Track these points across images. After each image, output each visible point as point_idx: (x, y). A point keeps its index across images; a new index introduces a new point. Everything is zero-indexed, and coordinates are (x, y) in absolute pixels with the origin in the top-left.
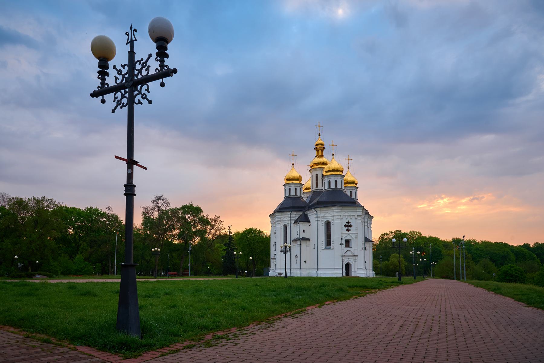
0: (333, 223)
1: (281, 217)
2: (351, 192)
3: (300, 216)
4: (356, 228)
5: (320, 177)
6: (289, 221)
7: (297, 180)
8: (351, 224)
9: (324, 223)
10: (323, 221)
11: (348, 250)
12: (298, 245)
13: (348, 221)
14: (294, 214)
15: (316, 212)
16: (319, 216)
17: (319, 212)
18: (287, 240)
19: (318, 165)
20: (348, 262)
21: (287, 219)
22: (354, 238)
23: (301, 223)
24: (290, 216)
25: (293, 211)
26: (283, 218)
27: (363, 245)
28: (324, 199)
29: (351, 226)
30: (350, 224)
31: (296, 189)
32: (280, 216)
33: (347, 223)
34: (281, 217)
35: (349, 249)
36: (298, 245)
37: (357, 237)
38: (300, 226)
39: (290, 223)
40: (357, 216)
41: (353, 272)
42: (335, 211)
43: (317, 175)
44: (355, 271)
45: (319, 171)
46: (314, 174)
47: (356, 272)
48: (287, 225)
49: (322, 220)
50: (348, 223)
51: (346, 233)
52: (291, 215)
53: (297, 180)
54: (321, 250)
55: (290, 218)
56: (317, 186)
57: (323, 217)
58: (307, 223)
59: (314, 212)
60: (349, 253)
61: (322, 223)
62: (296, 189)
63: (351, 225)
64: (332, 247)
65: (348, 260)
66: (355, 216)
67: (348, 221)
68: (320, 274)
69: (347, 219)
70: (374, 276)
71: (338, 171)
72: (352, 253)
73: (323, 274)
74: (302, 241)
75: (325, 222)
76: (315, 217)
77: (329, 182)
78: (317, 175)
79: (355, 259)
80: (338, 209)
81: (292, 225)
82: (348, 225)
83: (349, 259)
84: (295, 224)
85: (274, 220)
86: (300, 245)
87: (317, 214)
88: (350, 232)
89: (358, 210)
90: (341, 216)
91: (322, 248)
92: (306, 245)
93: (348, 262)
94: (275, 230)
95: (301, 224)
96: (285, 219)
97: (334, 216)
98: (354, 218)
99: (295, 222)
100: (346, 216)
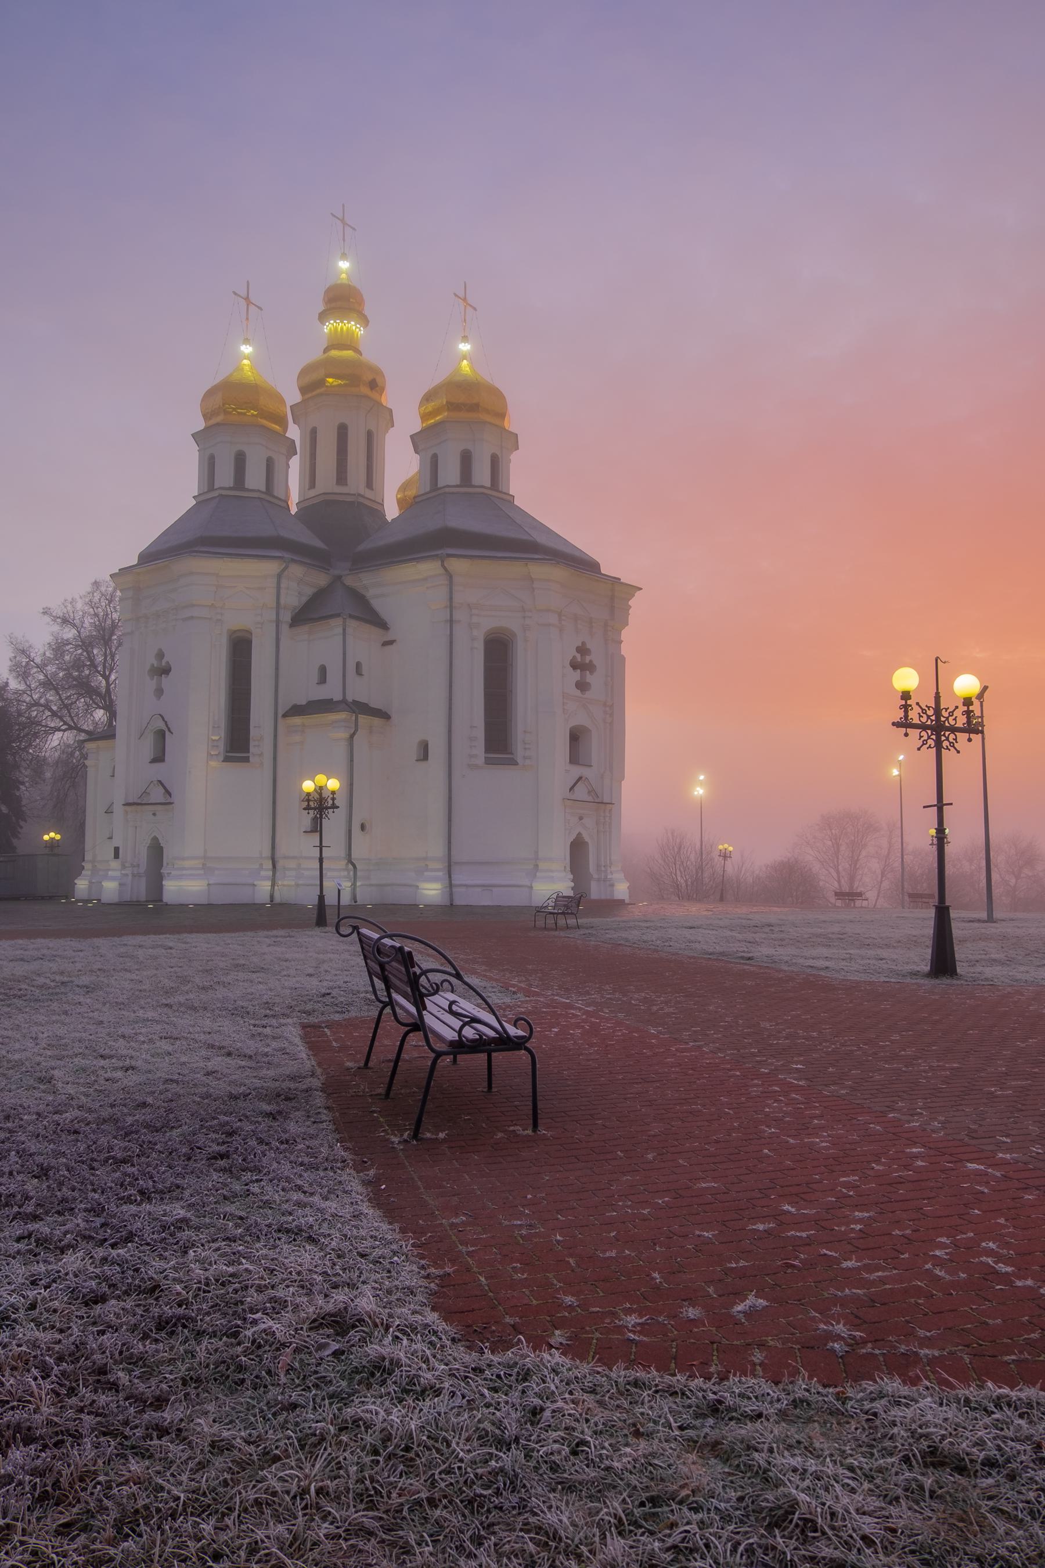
8: (596, 657)
9: (480, 635)
11: (580, 778)
13: (583, 643)
20: (579, 834)
25: (293, 561)
29: (589, 667)
30: (588, 659)
50: (582, 650)
56: (342, 477)
63: (591, 661)
64: (525, 758)
67: (583, 643)
68: (463, 889)
73: (479, 889)
81: (285, 628)
82: (581, 665)
83: (581, 818)
84: (306, 628)
88: (588, 695)
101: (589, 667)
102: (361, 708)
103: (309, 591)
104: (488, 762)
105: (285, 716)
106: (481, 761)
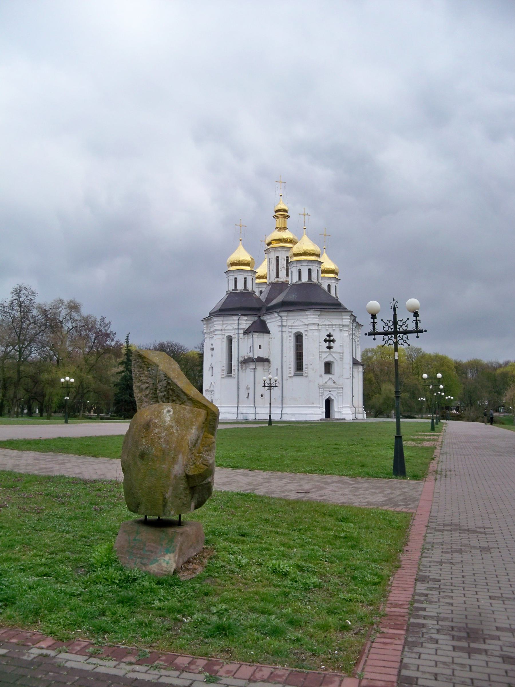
0: (306, 335)
1: (223, 324)
2: (329, 286)
3: (252, 323)
4: (341, 344)
5: (283, 263)
6: (237, 331)
7: (248, 264)
10: (291, 332)
12: (251, 369)
13: (330, 333)
14: (244, 320)
15: (279, 318)
16: (284, 324)
17: (285, 318)
18: (231, 361)
19: (279, 243)
20: (329, 397)
21: (232, 327)
22: (339, 360)
23: (256, 335)
24: (238, 323)
25: (242, 315)
26: (225, 326)
27: (350, 370)
28: (293, 298)
29: (333, 341)
31: (245, 278)
32: (221, 322)
33: (327, 336)
34: (223, 324)
35: (330, 376)
36: (251, 369)
37: (343, 359)
38: (255, 339)
39: (238, 334)
40: (343, 326)
41: (336, 412)
42: (310, 318)
43: (277, 257)
44: (339, 410)
45: (281, 252)
46: (273, 256)
47: (340, 412)
48: (231, 336)
49: (290, 330)
50: (329, 336)
51: (326, 352)
52: (240, 322)
53: (248, 264)
54: (288, 378)
55: (238, 325)
56: (277, 275)
57: (292, 326)
58: (265, 334)
59: (276, 317)
60: (330, 383)
61: (290, 336)
62: (245, 278)
63: (333, 339)
65: (328, 394)
66: (339, 325)
67: (330, 333)
68: (286, 415)
69: (327, 330)
70: (365, 417)
71: (313, 254)
72: (334, 383)
74: (257, 363)
75: (294, 334)
76: (279, 326)
77: (300, 271)
78: (277, 257)
79: (339, 392)
80: (313, 315)
81: (241, 336)
82: (330, 340)
84: (246, 335)
85: (211, 327)
86: (255, 369)
87: (282, 322)
88: (331, 350)
89: (344, 317)
90: (318, 325)
91: (290, 375)
92: (264, 370)
93: (329, 397)
94: (212, 344)
95: (256, 336)
96: (229, 327)
97: (308, 325)
98: (337, 329)
99: (247, 332)
100: (326, 325)
101: (333, 341)
102: (261, 360)
103: (251, 322)
104: (295, 375)
105: (241, 363)
106: (292, 375)
